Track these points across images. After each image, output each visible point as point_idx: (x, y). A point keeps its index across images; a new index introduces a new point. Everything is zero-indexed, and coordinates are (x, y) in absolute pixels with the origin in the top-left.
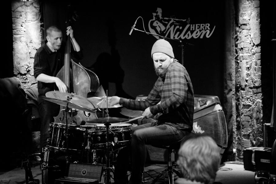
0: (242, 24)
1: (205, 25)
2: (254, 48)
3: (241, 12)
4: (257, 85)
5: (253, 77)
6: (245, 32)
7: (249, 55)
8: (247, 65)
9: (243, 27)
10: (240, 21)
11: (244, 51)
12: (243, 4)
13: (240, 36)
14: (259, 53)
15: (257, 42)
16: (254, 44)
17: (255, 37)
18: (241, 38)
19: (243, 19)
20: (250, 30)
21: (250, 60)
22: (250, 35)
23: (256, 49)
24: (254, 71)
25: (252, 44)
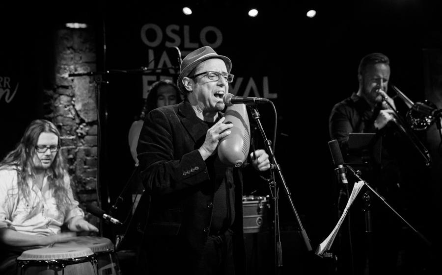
0: (60, 85)
1: (4, 79)
2: (81, 126)
3: (59, 65)
4: (89, 187)
5: (82, 175)
6: (64, 99)
7: (73, 139)
8: (69, 155)
9: (61, 90)
10: (57, 80)
11: (63, 131)
12: (61, 53)
13: (56, 105)
14: (94, 135)
15: (91, 117)
16: (82, 121)
17: (85, 110)
18: (58, 108)
19: (63, 78)
20: (73, 96)
21: (74, 147)
22: (74, 106)
23: (87, 129)
24: (83, 164)
25: (77, 121)
